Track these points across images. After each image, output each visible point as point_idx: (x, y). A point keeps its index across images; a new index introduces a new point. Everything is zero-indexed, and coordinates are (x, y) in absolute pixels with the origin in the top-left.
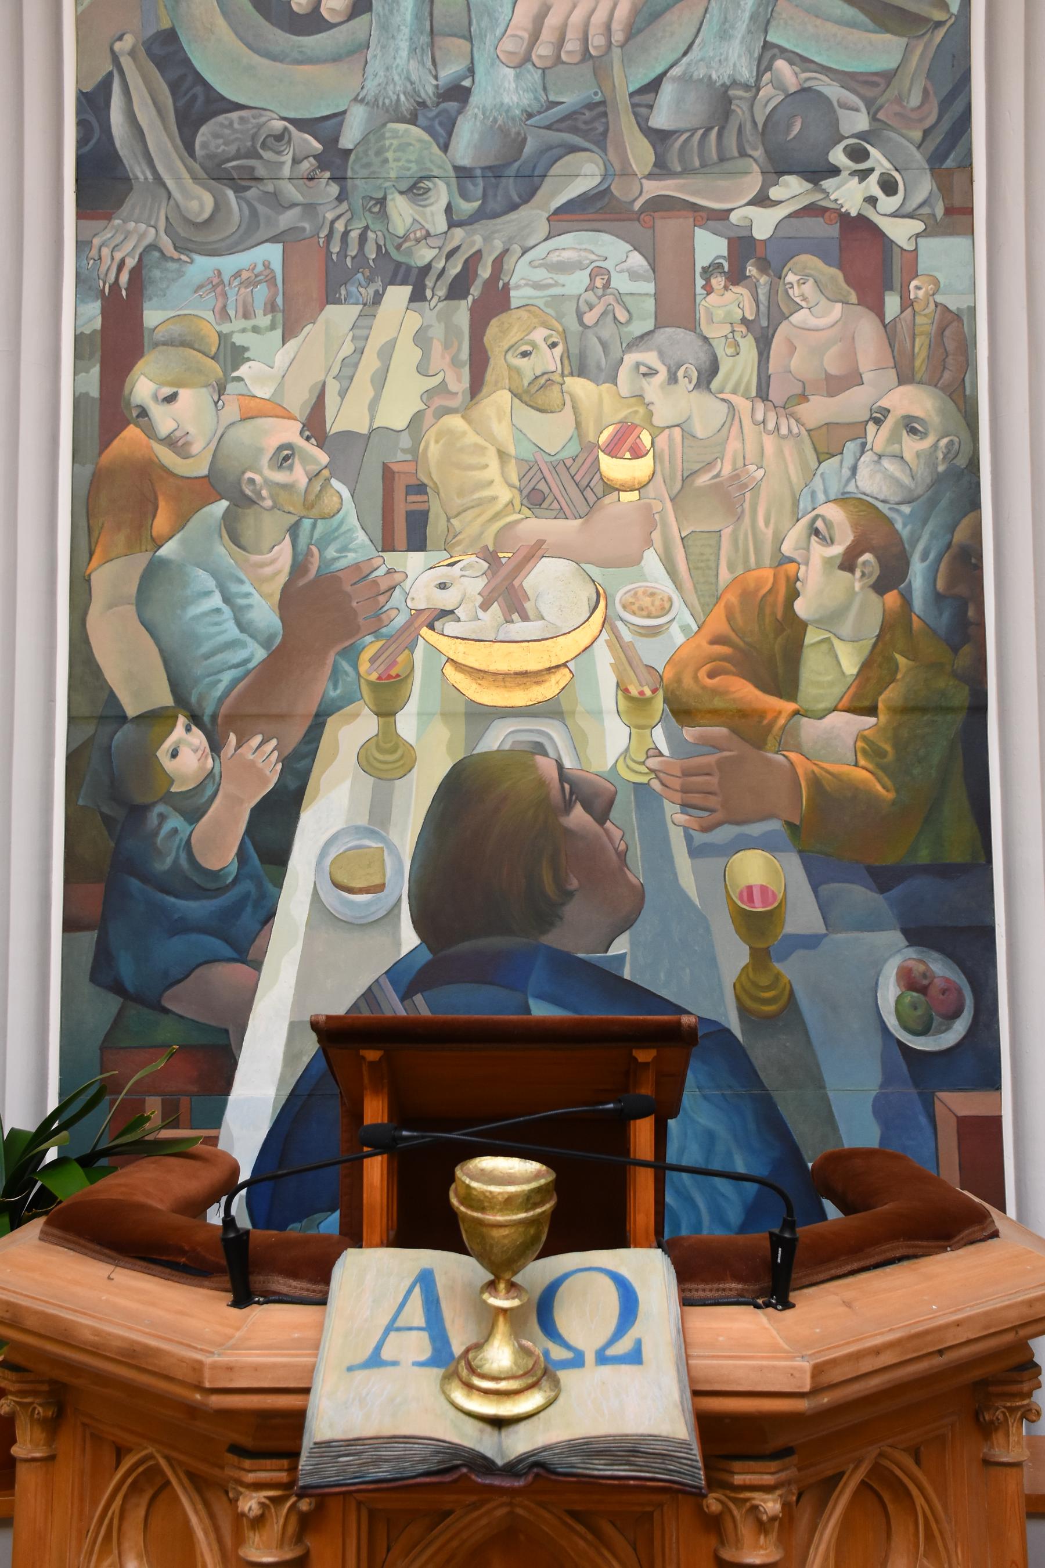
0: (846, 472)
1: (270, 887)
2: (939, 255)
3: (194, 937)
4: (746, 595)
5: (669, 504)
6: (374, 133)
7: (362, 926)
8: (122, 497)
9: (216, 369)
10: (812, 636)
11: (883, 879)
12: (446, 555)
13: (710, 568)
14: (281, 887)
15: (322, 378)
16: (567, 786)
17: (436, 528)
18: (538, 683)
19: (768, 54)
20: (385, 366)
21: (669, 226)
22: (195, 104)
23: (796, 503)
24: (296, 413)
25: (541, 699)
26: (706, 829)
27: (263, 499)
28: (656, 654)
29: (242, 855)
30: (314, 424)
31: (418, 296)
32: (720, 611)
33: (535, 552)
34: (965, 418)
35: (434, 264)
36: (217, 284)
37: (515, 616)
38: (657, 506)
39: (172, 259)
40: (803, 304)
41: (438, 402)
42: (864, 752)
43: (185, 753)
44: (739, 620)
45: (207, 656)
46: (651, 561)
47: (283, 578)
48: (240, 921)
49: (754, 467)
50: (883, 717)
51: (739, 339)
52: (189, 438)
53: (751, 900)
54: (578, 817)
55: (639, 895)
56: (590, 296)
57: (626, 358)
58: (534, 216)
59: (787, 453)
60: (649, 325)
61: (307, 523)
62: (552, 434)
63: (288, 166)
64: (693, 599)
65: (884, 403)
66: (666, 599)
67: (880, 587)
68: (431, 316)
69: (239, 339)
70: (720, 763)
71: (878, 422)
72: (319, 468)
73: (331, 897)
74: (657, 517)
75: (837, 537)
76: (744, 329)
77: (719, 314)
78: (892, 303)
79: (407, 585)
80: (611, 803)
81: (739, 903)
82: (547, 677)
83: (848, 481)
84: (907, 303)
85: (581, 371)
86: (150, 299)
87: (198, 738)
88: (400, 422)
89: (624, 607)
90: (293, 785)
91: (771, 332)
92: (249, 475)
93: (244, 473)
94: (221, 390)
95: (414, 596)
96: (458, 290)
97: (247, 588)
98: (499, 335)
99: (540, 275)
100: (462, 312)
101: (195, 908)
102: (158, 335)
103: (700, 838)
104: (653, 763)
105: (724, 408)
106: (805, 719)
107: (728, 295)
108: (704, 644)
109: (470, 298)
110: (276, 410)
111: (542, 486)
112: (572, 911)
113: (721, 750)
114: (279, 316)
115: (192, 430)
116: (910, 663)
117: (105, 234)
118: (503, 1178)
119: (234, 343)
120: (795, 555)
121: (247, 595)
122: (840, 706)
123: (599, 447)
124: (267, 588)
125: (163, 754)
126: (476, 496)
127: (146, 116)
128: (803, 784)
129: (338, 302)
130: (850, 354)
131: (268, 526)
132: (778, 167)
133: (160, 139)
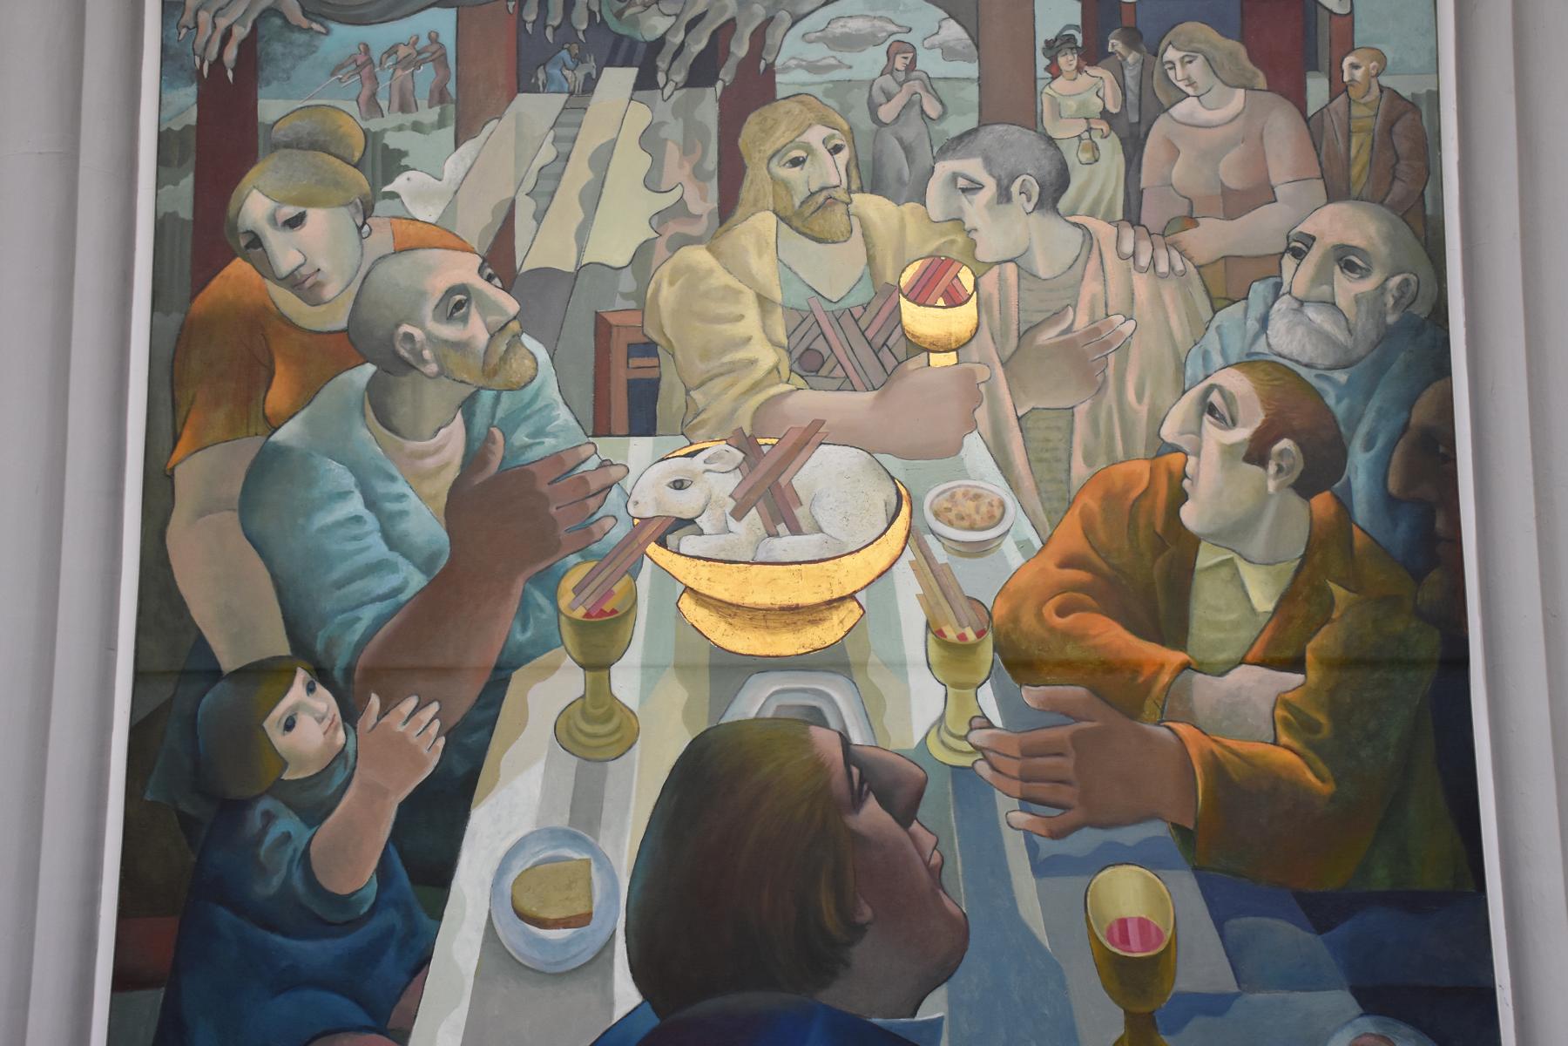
0: (1252, 325)
1: (425, 920)
3: (310, 995)
4: (1110, 498)
5: (999, 371)
7: (559, 977)
8: (223, 357)
9: (360, 180)
10: (1206, 557)
11: (1320, 912)
12: (683, 441)
13: (1058, 460)
14: (440, 918)
15: (511, 194)
16: (855, 771)
17: (670, 403)
18: (814, 622)
23: (1181, 368)
24: (473, 240)
25: (817, 645)
26: (1056, 835)
27: (425, 362)
28: (981, 582)
29: (383, 870)
30: (499, 258)
31: (646, 82)
32: (1073, 521)
33: (810, 437)
34: (1426, 246)
35: (668, 37)
36: (363, 63)
37: (782, 528)
38: (982, 373)
39: (300, 29)
40: (1189, 90)
41: (673, 228)
42: (1287, 725)
43: (306, 724)
44: (1102, 534)
45: (340, 584)
46: (975, 450)
47: (452, 473)
49: (1120, 318)
50: (1313, 674)
51: (1097, 140)
52: (320, 277)
53: (1125, 940)
54: (872, 815)
55: (961, 929)
56: (887, 82)
57: (937, 166)
59: (1167, 298)
60: (971, 121)
61: (487, 397)
62: (834, 272)
64: (1035, 502)
65: (1307, 227)
66: (995, 503)
68: (665, 110)
69: (393, 141)
70: (1076, 738)
71: (1299, 254)
72: (504, 320)
73: (513, 934)
74: (982, 388)
75: (1241, 416)
76: (1105, 127)
77: (1071, 105)
78: (1317, 89)
79: (628, 483)
80: (919, 795)
81: (1108, 945)
82: (826, 614)
83: (1256, 337)
84: (1338, 88)
85: (875, 185)
86: (268, 83)
87: (324, 701)
88: (620, 258)
89: (937, 515)
90: (460, 769)
91: (1143, 129)
92: (405, 328)
93: (398, 326)
94: (367, 210)
95: (639, 499)
96: (702, 73)
97: (400, 487)
98: (762, 136)
99: (818, 52)
100: (708, 106)
101: (314, 952)
102: (279, 134)
103: (1049, 847)
104: (978, 737)
105: (1077, 235)
106: (1199, 676)
107: (1083, 79)
108: (1051, 566)
109: (719, 85)
110: (445, 238)
111: (819, 344)
112: (861, 953)
113: (1078, 720)
114: (451, 108)
115: (324, 265)
116: (1352, 595)
119: (386, 146)
120: (1181, 442)
121: (401, 497)
122: (1249, 658)
123: (900, 291)
124: (428, 488)
125: (272, 724)
126: (727, 359)
128: (1198, 770)
129: (534, 89)
130: (1258, 159)
131: (433, 398)
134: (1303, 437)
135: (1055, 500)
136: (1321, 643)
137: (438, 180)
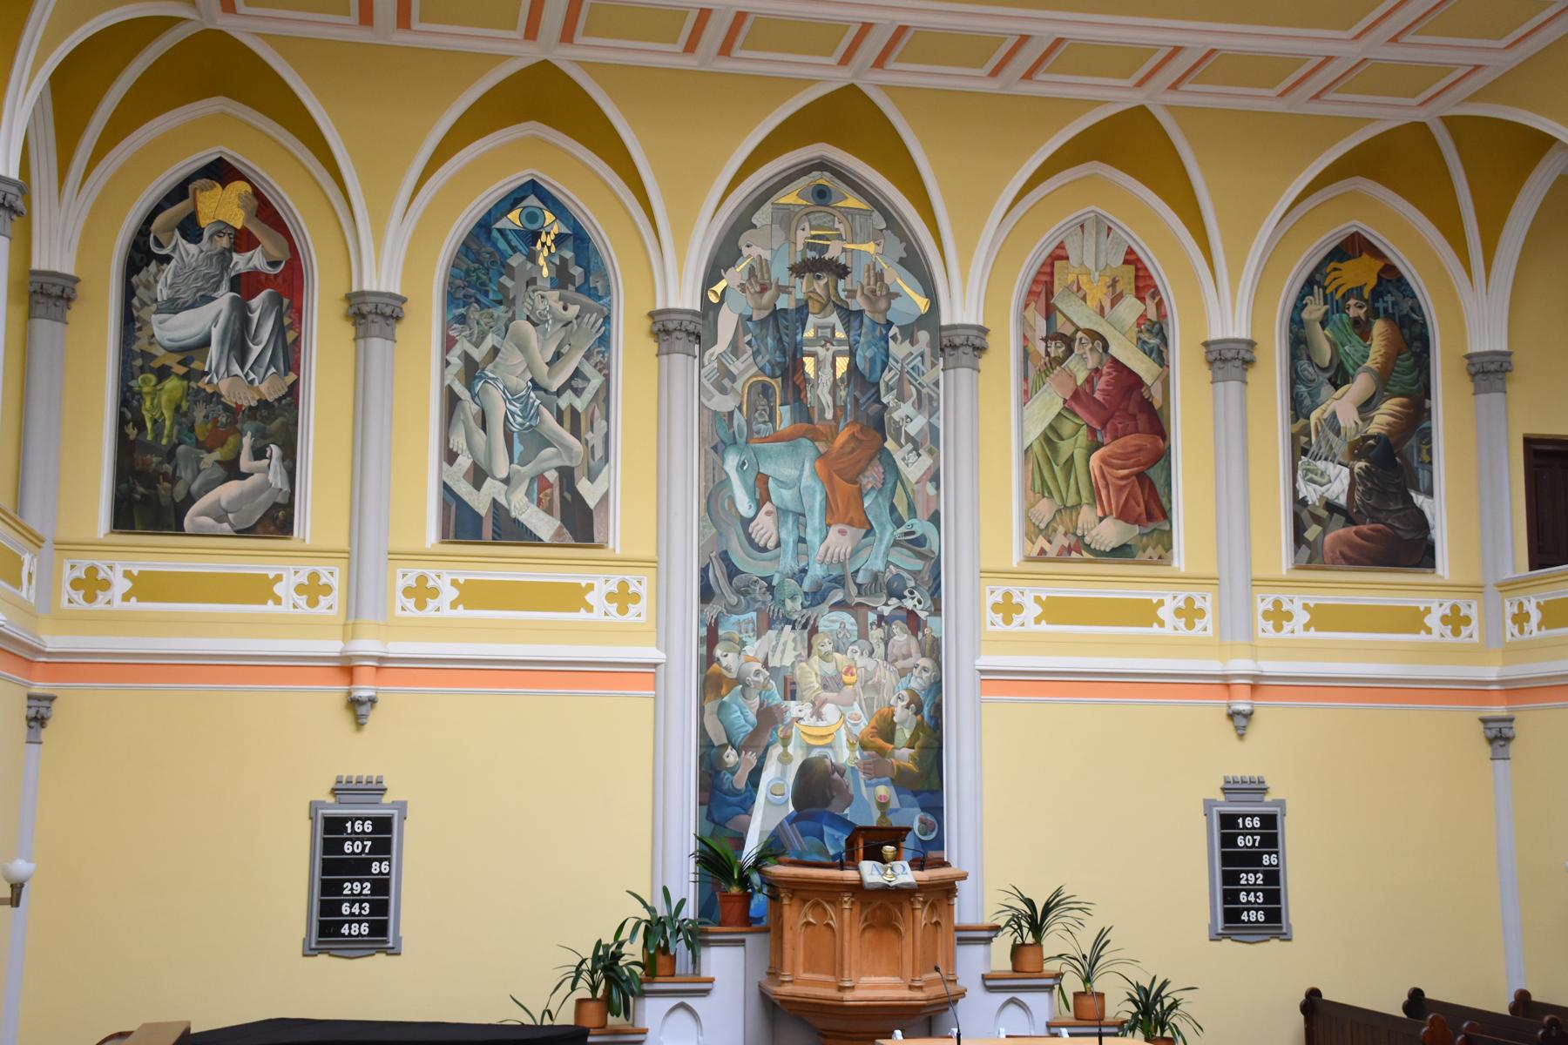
2: (932, 621)
6: (781, 583)
8: (712, 683)
11: (915, 794)
17: (798, 694)
19: (888, 563)
20: (784, 647)
21: (861, 611)
22: (732, 572)
28: (857, 731)
30: (765, 664)
33: (825, 702)
36: (738, 623)
46: (856, 705)
48: (746, 803)
54: (836, 775)
58: (825, 607)
62: (830, 669)
63: (758, 590)
67: (916, 714)
73: (771, 797)
96: (804, 627)
98: (816, 640)
110: (755, 660)
112: (835, 802)
117: (708, 608)
127: (719, 574)
131: (753, 692)
132: (890, 595)
133: (723, 582)
134: (916, 704)
135: (870, 715)
136: (918, 744)
137: (754, 647)
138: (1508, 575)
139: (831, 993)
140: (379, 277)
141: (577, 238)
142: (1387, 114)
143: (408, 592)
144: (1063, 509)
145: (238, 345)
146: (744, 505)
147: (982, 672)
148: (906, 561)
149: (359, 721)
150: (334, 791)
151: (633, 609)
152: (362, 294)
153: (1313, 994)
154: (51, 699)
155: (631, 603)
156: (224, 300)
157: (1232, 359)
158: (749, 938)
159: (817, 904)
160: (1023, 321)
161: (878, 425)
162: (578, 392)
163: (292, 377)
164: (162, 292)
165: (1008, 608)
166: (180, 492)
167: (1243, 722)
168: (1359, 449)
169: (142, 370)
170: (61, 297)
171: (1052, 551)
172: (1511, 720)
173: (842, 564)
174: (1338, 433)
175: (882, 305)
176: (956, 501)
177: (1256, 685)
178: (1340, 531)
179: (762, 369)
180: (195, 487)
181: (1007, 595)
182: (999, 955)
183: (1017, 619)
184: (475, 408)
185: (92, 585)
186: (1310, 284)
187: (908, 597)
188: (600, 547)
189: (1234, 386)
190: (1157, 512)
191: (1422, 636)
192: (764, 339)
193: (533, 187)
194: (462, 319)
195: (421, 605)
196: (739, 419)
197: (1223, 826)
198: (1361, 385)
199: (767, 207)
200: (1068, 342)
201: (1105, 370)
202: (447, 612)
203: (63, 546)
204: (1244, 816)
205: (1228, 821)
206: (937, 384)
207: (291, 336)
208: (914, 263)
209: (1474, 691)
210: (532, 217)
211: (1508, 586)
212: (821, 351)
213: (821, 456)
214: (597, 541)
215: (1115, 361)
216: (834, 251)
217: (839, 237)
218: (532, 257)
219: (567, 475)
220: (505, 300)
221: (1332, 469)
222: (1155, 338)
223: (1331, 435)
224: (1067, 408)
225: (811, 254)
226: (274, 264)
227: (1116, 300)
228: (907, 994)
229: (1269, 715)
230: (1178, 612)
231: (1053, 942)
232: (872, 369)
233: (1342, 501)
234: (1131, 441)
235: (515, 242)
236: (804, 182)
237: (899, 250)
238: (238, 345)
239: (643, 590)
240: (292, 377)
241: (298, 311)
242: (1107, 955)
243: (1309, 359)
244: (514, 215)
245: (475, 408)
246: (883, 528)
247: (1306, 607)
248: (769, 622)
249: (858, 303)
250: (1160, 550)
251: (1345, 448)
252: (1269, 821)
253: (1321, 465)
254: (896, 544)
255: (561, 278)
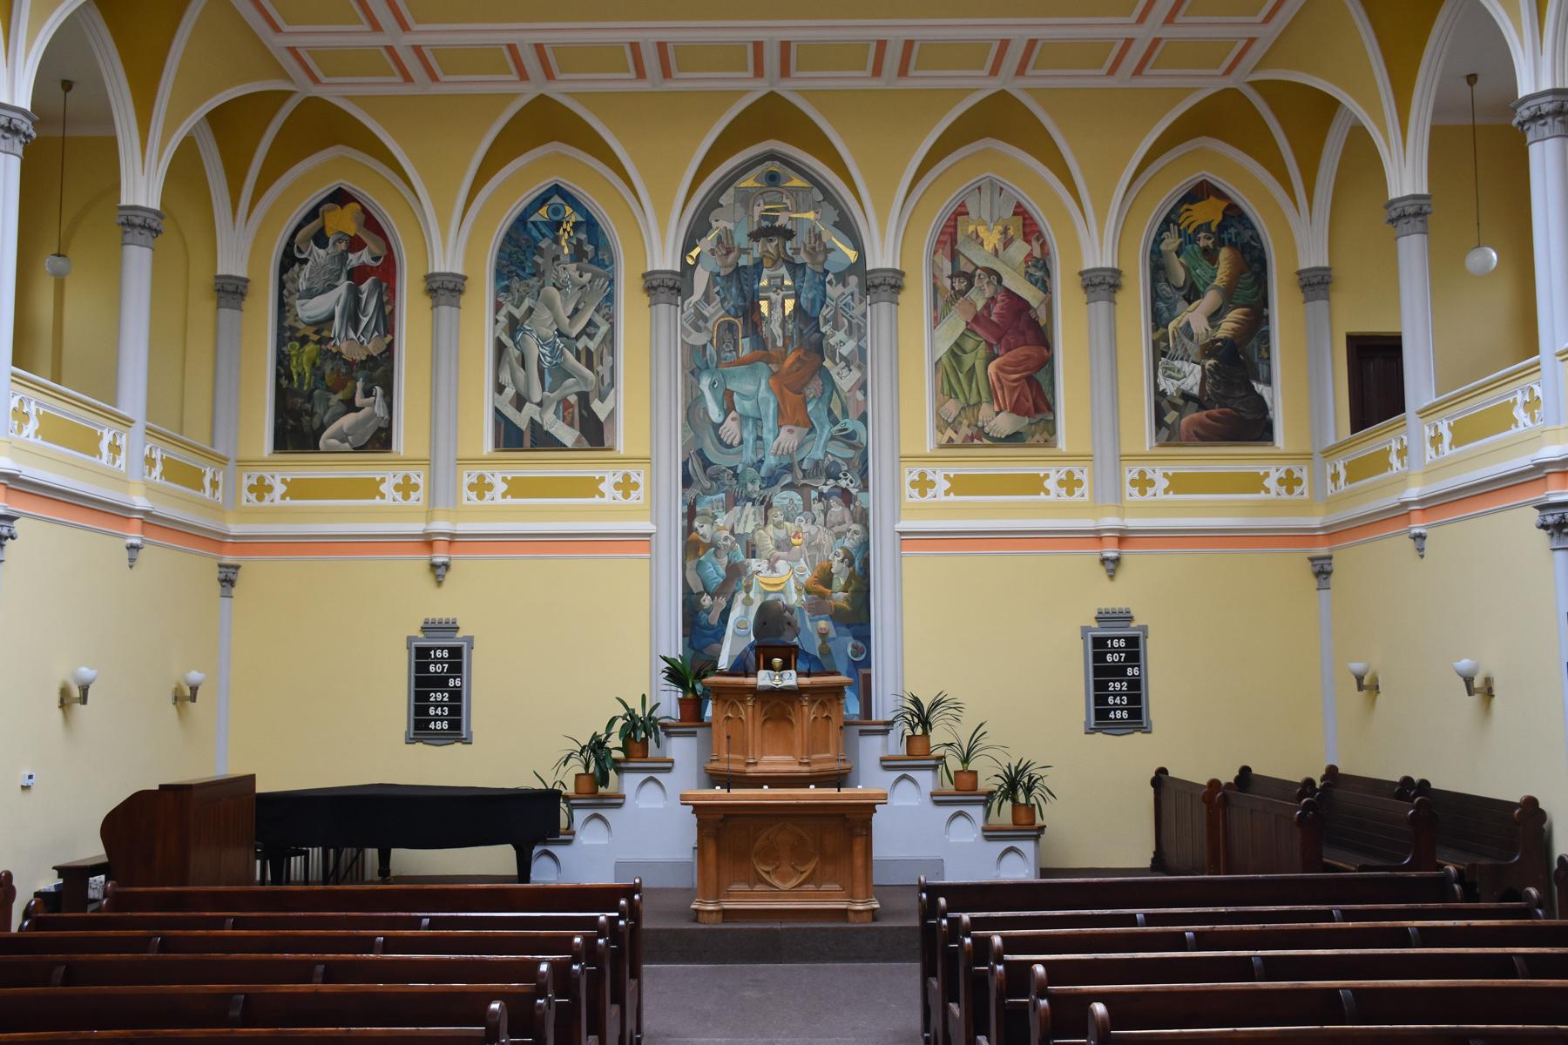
2: (861, 496)
8: (693, 547)
11: (848, 626)
19: (826, 453)
20: (747, 519)
21: (806, 490)
22: (706, 464)
28: (803, 580)
30: (732, 532)
33: (778, 559)
48: (719, 635)
58: (778, 488)
62: (782, 534)
63: (726, 477)
98: (771, 513)
101: (709, 632)
110: (724, 528)
117: (688, 492)
118: (777, 661)
131: (723, 553)
132: (828, 477)
134: (849, 558)
135: (813, 569)
137: (723, 520)
138: (1331, 442)
139: (740, 767)
140: (446, 261)
141: (590, 225)
142: (1208, 84)
143: (471, 487)
144: (967, 406)
145: (353, 318)
146: (715, 414)
147: (901, 533)
148: (841, 452)
149: (439, 582)
150: (424, 629)
151: (634, 494)
152: (433, 275)
153: (1162, 772)
154: (237, 567)
155: (631, 490)
156: (343, 286)
157: (1103, 284)
158: (698, 730)
159: (733, 704)
160: (934, 265)
161: (817, 349)
162: (591, 337)
163: (389, 338)
164: (303, 284)
165: (923, 485)
166: (316, 421)
167: (1111, 566)
168: (1209, 350)
169: (290, 339)
170: (234, 293)
171: (958, 439)
172: (1330, 558)
173: (790, 455)
174: (1191, 338)
175: (820, 258)
176: (878, 404)
177: (1123, 537)
178: (1193, 415)
179: (728, 312)
180: (326, 418)
181: (923, 475)
182: (894, 744)
183: (930, 493)
184: (517, 353)
185: (261, 489)
186: (1167, 222)
187: (842, 479)
188: (610, 449)
189: (1103, 305)
190: (1043, 406)
191: (1262, 495)
192: (729, 289)
193: (557, 189)
194: (507, 289)
195: (481, 496)
196: (711, 350)
197: (1095, 646)
198: (1210, 300)
199: (731, 191)
200: (970, 278)
201: (999, 298)
202: (499, 501)
203: (243, 463)
204: (1112, 639)
205: (1099, 643)
206: (864, 315)
207: (388, 309)
208: (846, 226)
209: (1302, 537)
210: (556, 211)
211: (1330, 452)
212: (773, 296)
213: (774, 374)
214: (607, 445)
215: (1008, 291)
216: (783, 220)
217: (787, 209)
218: (557, 241)
219: (584, 398)
220: (538, 273)
221: (1187, 367)
222: (1040, 272)
223: (1186, 340)
224: (969, 328)
225: (765, 224)
226: (376, 259)
227: (1007, 243)
228: (797, 768)
229: (1133, 559)
230: (1061, 483)
231: (938, 736)
232: (813, 306)
233: (1196, 391)
234: (1022, 351)
235: (544, 231)
236: (759, 170)
237: (834, 216)
238: (353, 318)
239: (641, 480)
240: (389, 338)
241: (392, 290)
242: (984, 742)
243: (1167, 281)
244: (543, 211)
245: (517, 353)
246: (822, 427)
247: (1166, 475)
248: (733, 501)
249: (802, 258)
250: (1046, 435)
251: (1197, 350)
252: (1133, 642)
253: (1178, 364)
254: (833, 438)
255: (578, 254)
